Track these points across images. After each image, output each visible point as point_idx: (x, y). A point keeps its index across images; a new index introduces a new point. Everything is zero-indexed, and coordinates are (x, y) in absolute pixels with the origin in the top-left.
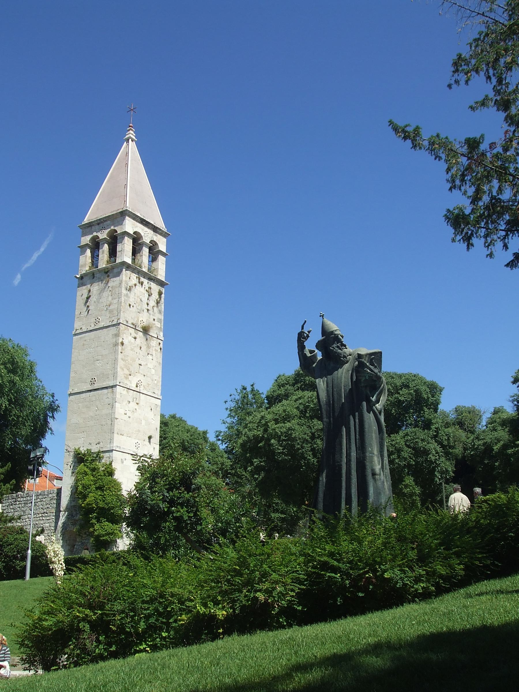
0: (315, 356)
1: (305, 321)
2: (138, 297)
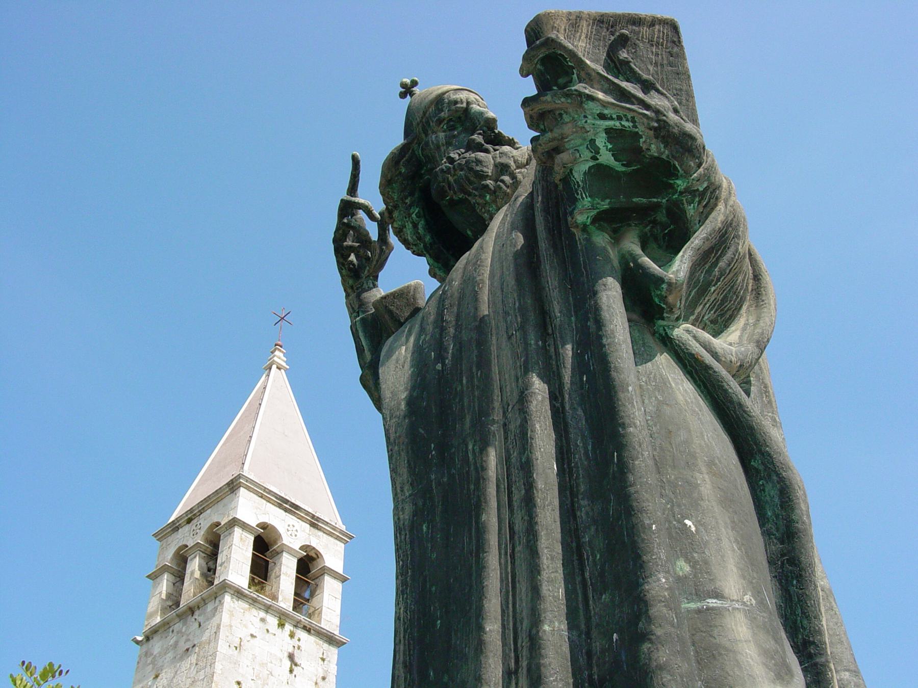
2: (263, 665)
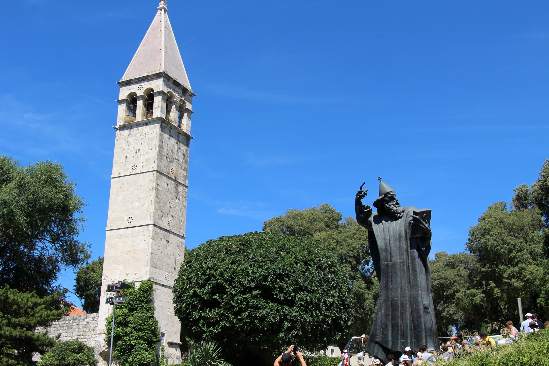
0: (370, 212)
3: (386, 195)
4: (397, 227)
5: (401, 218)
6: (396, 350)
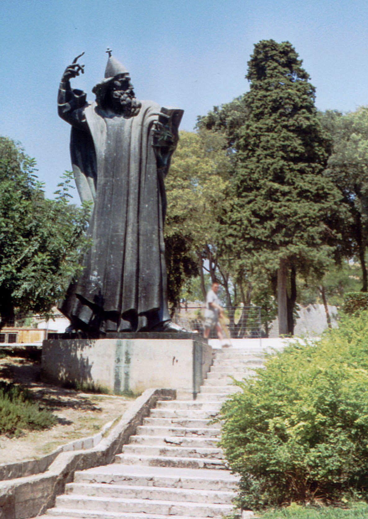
1: (83, 53)
3: (117, 78)
4: (132, 127)
5: (136, 115)
6: (112, 309)
